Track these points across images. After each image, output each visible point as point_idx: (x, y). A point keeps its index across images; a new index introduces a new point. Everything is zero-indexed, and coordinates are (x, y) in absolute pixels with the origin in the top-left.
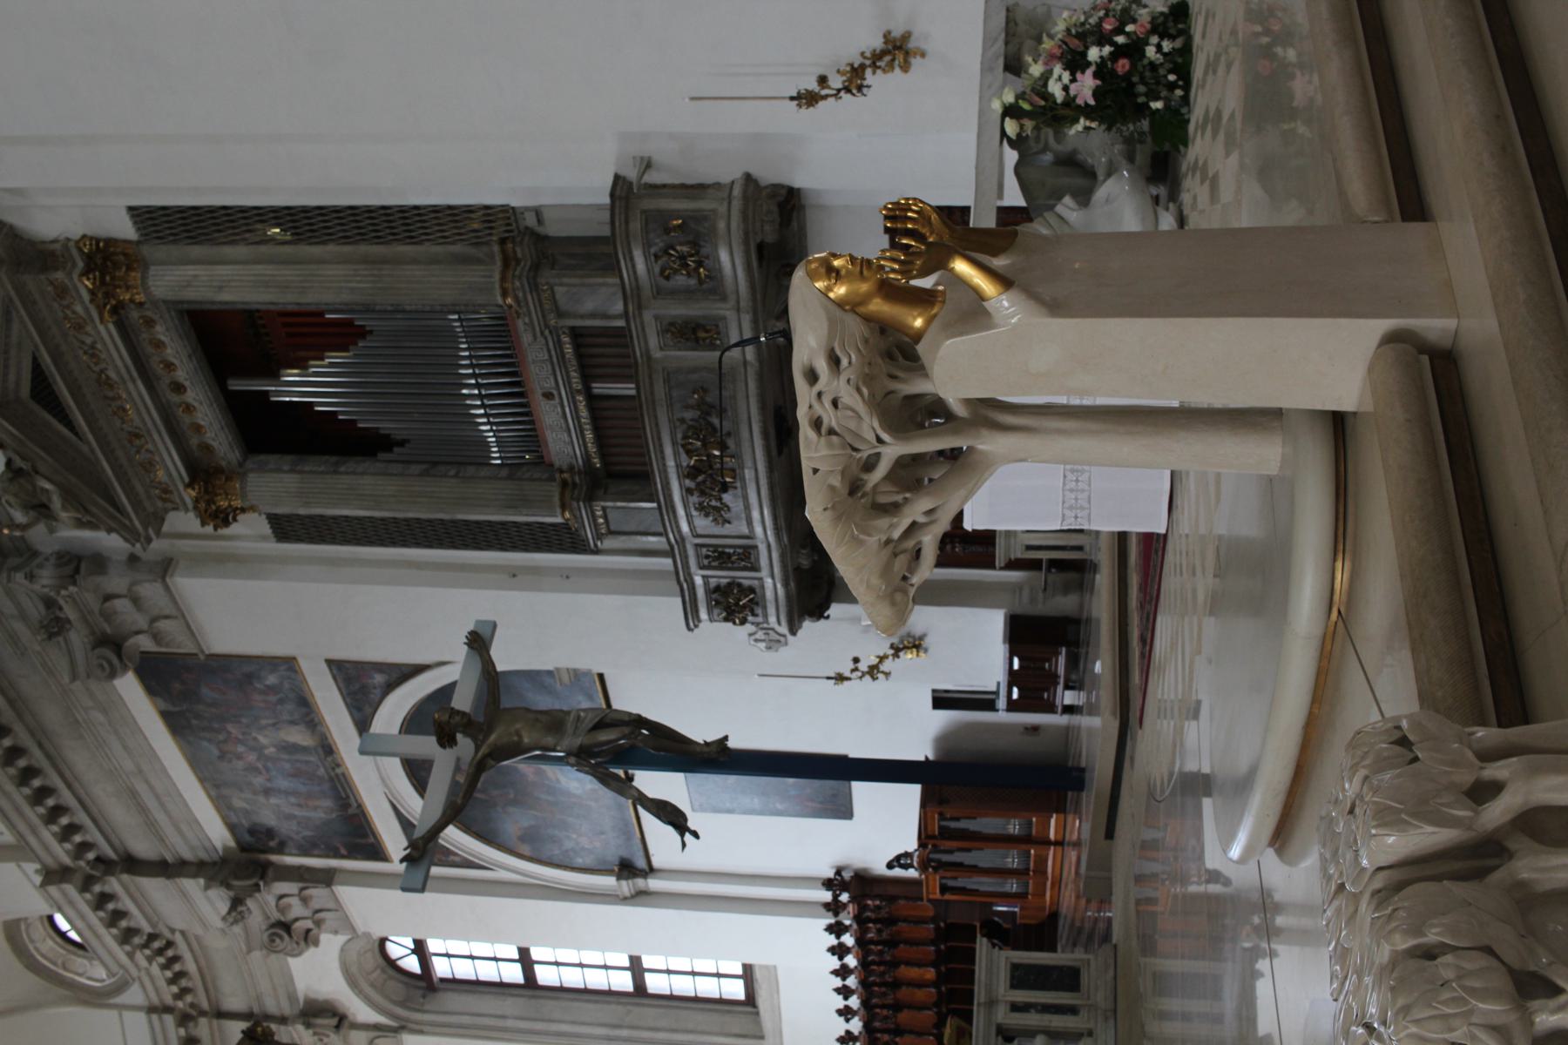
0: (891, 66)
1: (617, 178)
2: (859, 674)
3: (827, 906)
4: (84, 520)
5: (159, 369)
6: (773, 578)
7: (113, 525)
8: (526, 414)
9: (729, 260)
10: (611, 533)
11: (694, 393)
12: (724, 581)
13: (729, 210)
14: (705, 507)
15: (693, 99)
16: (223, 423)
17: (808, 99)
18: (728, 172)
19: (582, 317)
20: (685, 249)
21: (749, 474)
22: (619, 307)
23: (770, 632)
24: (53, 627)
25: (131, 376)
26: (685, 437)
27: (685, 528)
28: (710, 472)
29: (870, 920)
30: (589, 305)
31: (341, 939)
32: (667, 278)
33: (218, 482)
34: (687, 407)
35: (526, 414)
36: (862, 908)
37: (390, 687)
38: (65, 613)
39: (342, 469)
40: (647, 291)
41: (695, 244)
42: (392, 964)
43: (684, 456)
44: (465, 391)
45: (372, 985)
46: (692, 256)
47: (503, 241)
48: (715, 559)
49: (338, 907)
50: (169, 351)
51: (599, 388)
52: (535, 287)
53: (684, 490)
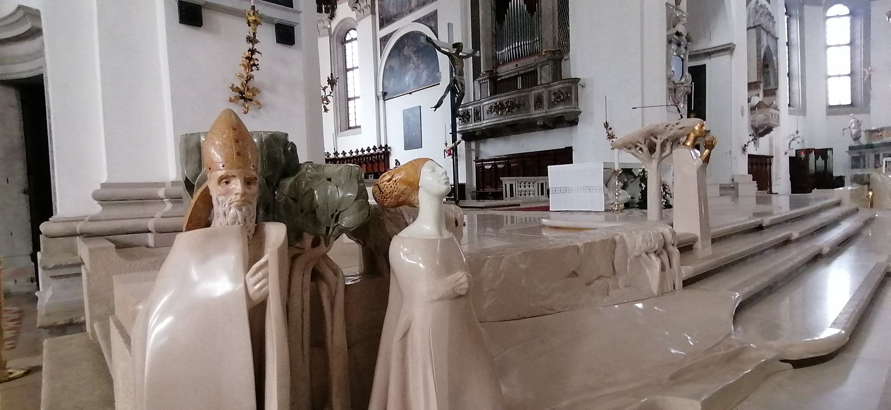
1: (579, 79)
3: (381, 146)
9: (559, 109)
10: (481, 84)
12: (470, 114)
17: (606, 125)
18: (581, 107)
19: (540, 73)
20: (562, 98)
21: (502, 118)
22: (543, 82)
26: (511, 101)
29: (378, 156)
31: (355, 18)
32: (554, 94)
34: (519, 101)
36: (381, 154)
37: (431, 28)
40: (549, 89)
41: (563, 100)
42: (348, 32)
44: (517, 43)
45: (342, 27)
47: (560, 50)
48: (477, 111)
49: (365, 16)
51: (519, 79)
52: (549, 60)
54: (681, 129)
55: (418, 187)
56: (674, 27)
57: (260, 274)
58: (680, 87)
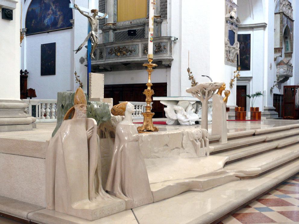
0: (192, 83)
13: (168, 56)
17: (189, 70)
27: (108, 46)
54: (216, 86)
55: (125, 110)
56: (229, 13)
57: (91, 131)
58: (232, 50)
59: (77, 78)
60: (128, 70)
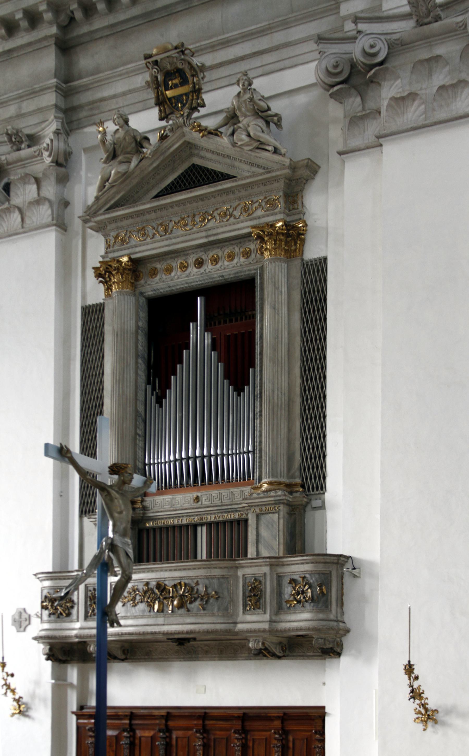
2: (5, 677)
4: (107, 184)
5: (213, 253)
6: (81, 629)
7: (101, 201)
8: (182, 485)
11: (216, 592)
14: (135, 592)
15: (410, 608)
16: (174, 288)
19: (257, 528)
20: (309, 594)
21: (161, 620)
23: (27, 622)
24: (15, 139)
25: (210, 236)
26: (186, 585)
28: (161, 597)
30: (264, 533)
32: (290, 583)
33: (130, 277)
34: (206, 588)
35: (182, 485)
38: (24, 149)
39: (140, 361)
40: (280, 570)
43: (172, 583)
46: (304, 598)
50: (226, 263)
51: (202, 533)
52: (278, 502)
53: (148, 580)
59: (6, 680)
60: (185, 659)
